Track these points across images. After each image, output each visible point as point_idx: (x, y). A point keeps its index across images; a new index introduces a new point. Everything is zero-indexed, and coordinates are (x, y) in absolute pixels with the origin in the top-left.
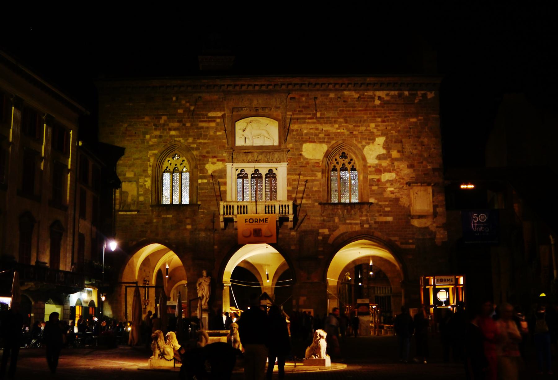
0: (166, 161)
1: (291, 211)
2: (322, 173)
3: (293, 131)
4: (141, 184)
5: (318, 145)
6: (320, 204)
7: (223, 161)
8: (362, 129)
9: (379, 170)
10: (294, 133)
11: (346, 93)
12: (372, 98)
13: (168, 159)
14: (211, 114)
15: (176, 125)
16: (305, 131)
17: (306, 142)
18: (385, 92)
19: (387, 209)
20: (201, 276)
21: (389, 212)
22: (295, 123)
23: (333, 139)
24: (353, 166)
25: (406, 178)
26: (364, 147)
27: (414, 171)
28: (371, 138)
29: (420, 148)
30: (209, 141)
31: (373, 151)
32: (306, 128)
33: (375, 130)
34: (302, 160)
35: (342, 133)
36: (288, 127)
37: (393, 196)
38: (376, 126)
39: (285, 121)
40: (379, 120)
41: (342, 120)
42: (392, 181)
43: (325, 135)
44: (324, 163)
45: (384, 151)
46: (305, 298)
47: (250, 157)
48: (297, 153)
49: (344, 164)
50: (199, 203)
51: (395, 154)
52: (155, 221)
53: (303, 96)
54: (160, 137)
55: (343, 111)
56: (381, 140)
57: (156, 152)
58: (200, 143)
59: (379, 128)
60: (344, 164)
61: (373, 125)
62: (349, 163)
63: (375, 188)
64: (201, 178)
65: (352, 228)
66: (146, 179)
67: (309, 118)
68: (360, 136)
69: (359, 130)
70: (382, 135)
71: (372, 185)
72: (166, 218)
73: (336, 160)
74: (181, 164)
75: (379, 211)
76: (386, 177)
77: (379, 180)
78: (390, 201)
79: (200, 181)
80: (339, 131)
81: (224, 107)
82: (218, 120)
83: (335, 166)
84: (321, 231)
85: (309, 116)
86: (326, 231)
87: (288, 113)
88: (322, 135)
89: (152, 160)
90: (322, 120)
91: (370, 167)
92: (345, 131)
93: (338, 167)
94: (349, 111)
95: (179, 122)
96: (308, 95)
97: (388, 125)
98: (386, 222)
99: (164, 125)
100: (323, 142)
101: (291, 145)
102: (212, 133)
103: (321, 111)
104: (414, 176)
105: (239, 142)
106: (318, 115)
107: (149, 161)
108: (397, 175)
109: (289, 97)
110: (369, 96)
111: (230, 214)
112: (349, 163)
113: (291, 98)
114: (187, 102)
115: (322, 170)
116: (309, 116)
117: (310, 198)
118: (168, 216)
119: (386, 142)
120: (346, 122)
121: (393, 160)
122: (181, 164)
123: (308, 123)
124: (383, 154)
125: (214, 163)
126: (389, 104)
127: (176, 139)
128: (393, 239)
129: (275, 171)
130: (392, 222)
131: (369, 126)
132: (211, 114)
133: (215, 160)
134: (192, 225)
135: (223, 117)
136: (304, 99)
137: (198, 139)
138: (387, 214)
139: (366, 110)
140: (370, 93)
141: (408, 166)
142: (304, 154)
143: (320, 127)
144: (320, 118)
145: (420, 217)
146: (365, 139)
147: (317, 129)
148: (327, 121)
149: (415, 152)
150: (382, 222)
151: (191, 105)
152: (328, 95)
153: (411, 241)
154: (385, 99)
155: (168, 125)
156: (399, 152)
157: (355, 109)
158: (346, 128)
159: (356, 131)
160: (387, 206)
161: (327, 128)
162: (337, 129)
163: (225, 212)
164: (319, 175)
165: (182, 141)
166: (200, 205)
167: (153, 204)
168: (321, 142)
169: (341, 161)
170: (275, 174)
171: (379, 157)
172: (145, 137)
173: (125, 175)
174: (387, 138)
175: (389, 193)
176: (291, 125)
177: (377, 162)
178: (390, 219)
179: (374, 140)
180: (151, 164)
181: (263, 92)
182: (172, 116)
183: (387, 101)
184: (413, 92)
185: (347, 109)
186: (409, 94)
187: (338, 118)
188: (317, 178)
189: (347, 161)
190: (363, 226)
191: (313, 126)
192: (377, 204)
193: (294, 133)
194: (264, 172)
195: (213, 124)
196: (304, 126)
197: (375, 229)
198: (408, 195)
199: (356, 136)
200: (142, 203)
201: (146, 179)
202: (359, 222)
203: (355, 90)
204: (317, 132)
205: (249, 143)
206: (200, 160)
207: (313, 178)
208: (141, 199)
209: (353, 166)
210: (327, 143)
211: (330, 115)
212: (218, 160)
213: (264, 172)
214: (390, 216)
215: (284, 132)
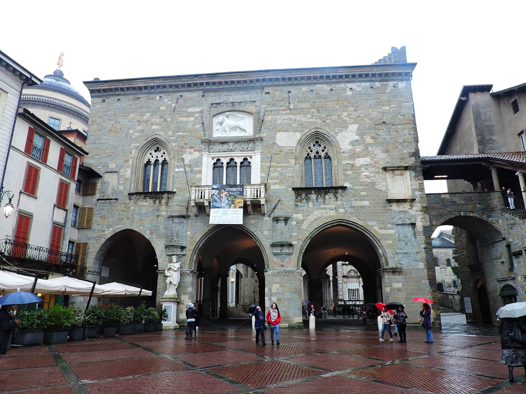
0: (149, 154)
1: (263, 195)
2: (296, 159)
3: (267, 122)
4: (121, 174)
5: (291, 134)
6: (294, 189)
7: (199, 151)
8: (335, 118)
9: (353, 155)
10: (269, 124)
11: (318, 86)
12: (345, 90)
13: (150, 151)
14: (190, 110)
15: (158, 120)
16: (279, 122)
17: (279, 131)
18: (357, 84)
19: (363, 193)
20: (171, 261)
21: (364, 196)
22: (269, 115)
23: (306, 127)
24: (327, 154)
25: (381, 163)
26: (337, 133)
27: (389, 155)
28: (344, 126)
29: (395, 133)
30: (187, 134)
31: (346, 138)
32: (280, 119)
33: (348, 118)
34: (276, 148)
35: (315, 122)
36: (261, 118)
37: (368, 180)
38: (349, 115)
39: (258, 113)
40: (352, 108)
41: (315, 110)
42: (367, 165)
43: (299, 125)
44: (298, 151)
45: (358, 138)
46: (278, 286)
47: (225, 146)
48: (271, 142)
49: (317, 153)
50: (174, 190)
51: (368, 140)
52: (132, 208)
53: (276, 91)
54: (143, 131)
55: (316, 102)
56: (354, 127)
57: (138, 144)
58: (179, 135)
59: (351, 116)
60: (317, 153)
61: (345, 114)
62: (323, 151)
63: (348, 173)
64: (178, 167)
65: (326, 213)
66: (127, 170)
67: (283, 110)
68: (332, 124)
69: (331, 119)
70: (354, 123)
71: (347, 170)
72: (143, 205)
73: (309, 148)
74: (162, 156)
75: (355, 196)
76: (360, 161)
77: (353, 166)
78: (365, 185)
79: (176, 170)
80: (312, 120)
81: (203, 104)
82: (197, 115)
83: (308, 155)
84: (294, 216)
85: (283, 108)
86: (300, 216)
87: (262, 106)
88: (294, 125)
89: (133, 152)
90: (294, 111)
91: (343, 152)
92: (318, 120)
93: (312, 155)
94: (321, 102)
95: (160, 118)
96: (282, 90)
97: (361, 114)
98: (362, 207)
99: (147, 121)
100: (297, 131)
101: (265, 134)
102: (190, 127)
103: (294, 103)
104: (390, 160)
105: (217, 134)
106: (292, 106)
107: (131, 153)
108: (371, 160)
109: (264, 92)
110: (340, 87)
111: (201, 198)
112: (323, 151)
113: (266, 93)
114: (169, 101)
115: (296, 156)
116: (283, 108)
117: (283, 184)
118: (145, 204)
119: (359, 129)
120: (319, 112)
121: (367, 146)
122: (162, 156)
123: (281, 114)
124: (356, 141)
125: (191, 153)
126: (361, 94)
127: (157, 133)
128: (370, 223)
129: (249, 160)
130: (369, 207)
131: (341, 115)
132: (190, 110)
133: (193, 150)
134: (167, 212)
135: (201, 112)
136: (278, 93)
137: (178, 132)
138: (363, 198)
139: (338, 101)
140: (342, 85)
141: (382, 151)
142: (277, 142)
143: (293, 117)
144: (294, 109)
145: (398, 201)
146: (338, 127)
147: (291, 119)
148: (300, 112)
149: (388, 137)
150: (358, 207)
151: (173, 103)
152: (301, 89)
153: (389, 226)
154: (357, 90)
155: (150, 120)
156: (372, 138)
157: (329, 100)
158: (319, 118)
159: (328, 119)
160: (363, 190)
161: (300, 118)
162: (310, 118)
163: (197, 196)
164: (293, 161)
165: (162, 134)
166: (175, 192)
167: (132, 191)
168: (294, 131)
169: (315, 149)
170: (249, 163)
171: (352, 143)
172: (128, 131)
173: (108, 166)
174: (360, 125)
175: (364, 177)
176: (265, 118)
177: (350, 147)
178: (366, 203)
179: (347, 127)
180: (133, 155)
181: (240, 89)
182: (154, 113)
183: (359, 91)
184: (385, 83)
185: (320, 100)
186: (381, 85)
187: (311, 109)
188: (291, 164)
189: (321, 148)
190: (338, 211)
191: (286, 117)
192: (352, 189)
193: (269, 124)
194: (238, 161)
195: (192, 119)
196: (278, 117)
197: (351, 213)
198: (385, 179)
199: (329, 125)
200: (121, 192)
201: (127, 170)
202: (334, 207)
203: (327, 83)
204: (290, 122)
205: (224, 135)
206: (178, 151)
207: (287, 164)
208: (121, 188)
209: (327, 154)
210: (300, 131)
211: (304, 105)
212: (195, 151)
213: (238, 161)
214: (366, 200)
215: (259, 123)
